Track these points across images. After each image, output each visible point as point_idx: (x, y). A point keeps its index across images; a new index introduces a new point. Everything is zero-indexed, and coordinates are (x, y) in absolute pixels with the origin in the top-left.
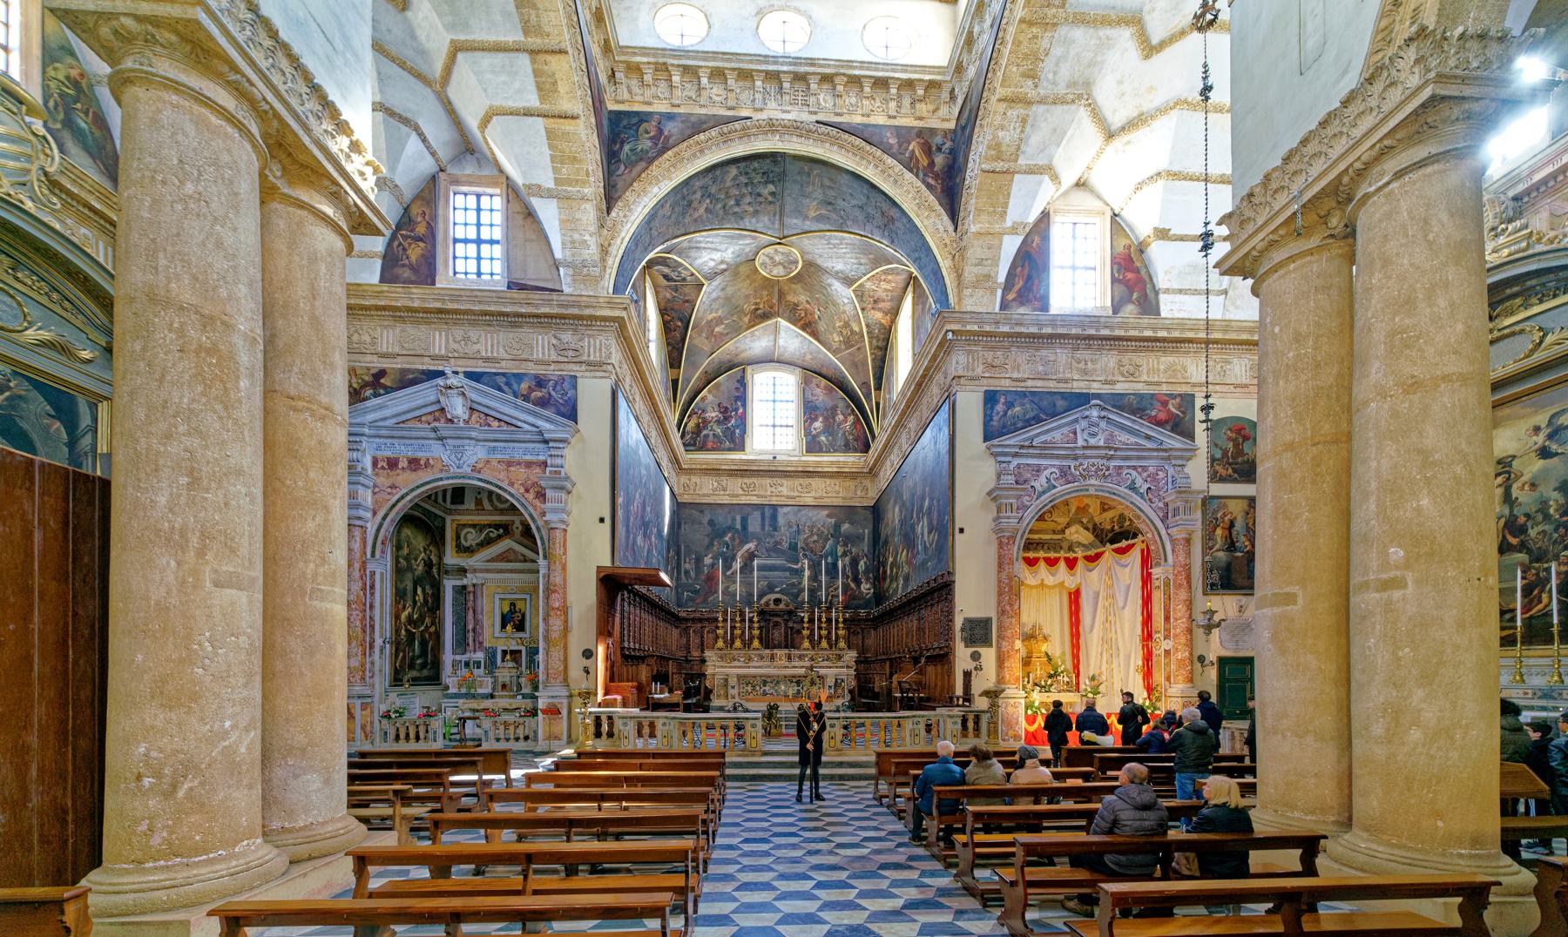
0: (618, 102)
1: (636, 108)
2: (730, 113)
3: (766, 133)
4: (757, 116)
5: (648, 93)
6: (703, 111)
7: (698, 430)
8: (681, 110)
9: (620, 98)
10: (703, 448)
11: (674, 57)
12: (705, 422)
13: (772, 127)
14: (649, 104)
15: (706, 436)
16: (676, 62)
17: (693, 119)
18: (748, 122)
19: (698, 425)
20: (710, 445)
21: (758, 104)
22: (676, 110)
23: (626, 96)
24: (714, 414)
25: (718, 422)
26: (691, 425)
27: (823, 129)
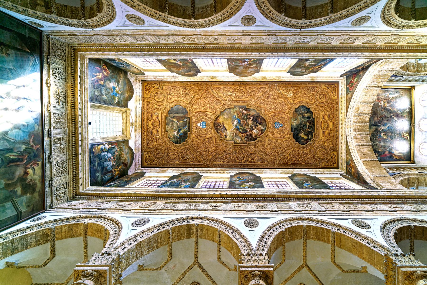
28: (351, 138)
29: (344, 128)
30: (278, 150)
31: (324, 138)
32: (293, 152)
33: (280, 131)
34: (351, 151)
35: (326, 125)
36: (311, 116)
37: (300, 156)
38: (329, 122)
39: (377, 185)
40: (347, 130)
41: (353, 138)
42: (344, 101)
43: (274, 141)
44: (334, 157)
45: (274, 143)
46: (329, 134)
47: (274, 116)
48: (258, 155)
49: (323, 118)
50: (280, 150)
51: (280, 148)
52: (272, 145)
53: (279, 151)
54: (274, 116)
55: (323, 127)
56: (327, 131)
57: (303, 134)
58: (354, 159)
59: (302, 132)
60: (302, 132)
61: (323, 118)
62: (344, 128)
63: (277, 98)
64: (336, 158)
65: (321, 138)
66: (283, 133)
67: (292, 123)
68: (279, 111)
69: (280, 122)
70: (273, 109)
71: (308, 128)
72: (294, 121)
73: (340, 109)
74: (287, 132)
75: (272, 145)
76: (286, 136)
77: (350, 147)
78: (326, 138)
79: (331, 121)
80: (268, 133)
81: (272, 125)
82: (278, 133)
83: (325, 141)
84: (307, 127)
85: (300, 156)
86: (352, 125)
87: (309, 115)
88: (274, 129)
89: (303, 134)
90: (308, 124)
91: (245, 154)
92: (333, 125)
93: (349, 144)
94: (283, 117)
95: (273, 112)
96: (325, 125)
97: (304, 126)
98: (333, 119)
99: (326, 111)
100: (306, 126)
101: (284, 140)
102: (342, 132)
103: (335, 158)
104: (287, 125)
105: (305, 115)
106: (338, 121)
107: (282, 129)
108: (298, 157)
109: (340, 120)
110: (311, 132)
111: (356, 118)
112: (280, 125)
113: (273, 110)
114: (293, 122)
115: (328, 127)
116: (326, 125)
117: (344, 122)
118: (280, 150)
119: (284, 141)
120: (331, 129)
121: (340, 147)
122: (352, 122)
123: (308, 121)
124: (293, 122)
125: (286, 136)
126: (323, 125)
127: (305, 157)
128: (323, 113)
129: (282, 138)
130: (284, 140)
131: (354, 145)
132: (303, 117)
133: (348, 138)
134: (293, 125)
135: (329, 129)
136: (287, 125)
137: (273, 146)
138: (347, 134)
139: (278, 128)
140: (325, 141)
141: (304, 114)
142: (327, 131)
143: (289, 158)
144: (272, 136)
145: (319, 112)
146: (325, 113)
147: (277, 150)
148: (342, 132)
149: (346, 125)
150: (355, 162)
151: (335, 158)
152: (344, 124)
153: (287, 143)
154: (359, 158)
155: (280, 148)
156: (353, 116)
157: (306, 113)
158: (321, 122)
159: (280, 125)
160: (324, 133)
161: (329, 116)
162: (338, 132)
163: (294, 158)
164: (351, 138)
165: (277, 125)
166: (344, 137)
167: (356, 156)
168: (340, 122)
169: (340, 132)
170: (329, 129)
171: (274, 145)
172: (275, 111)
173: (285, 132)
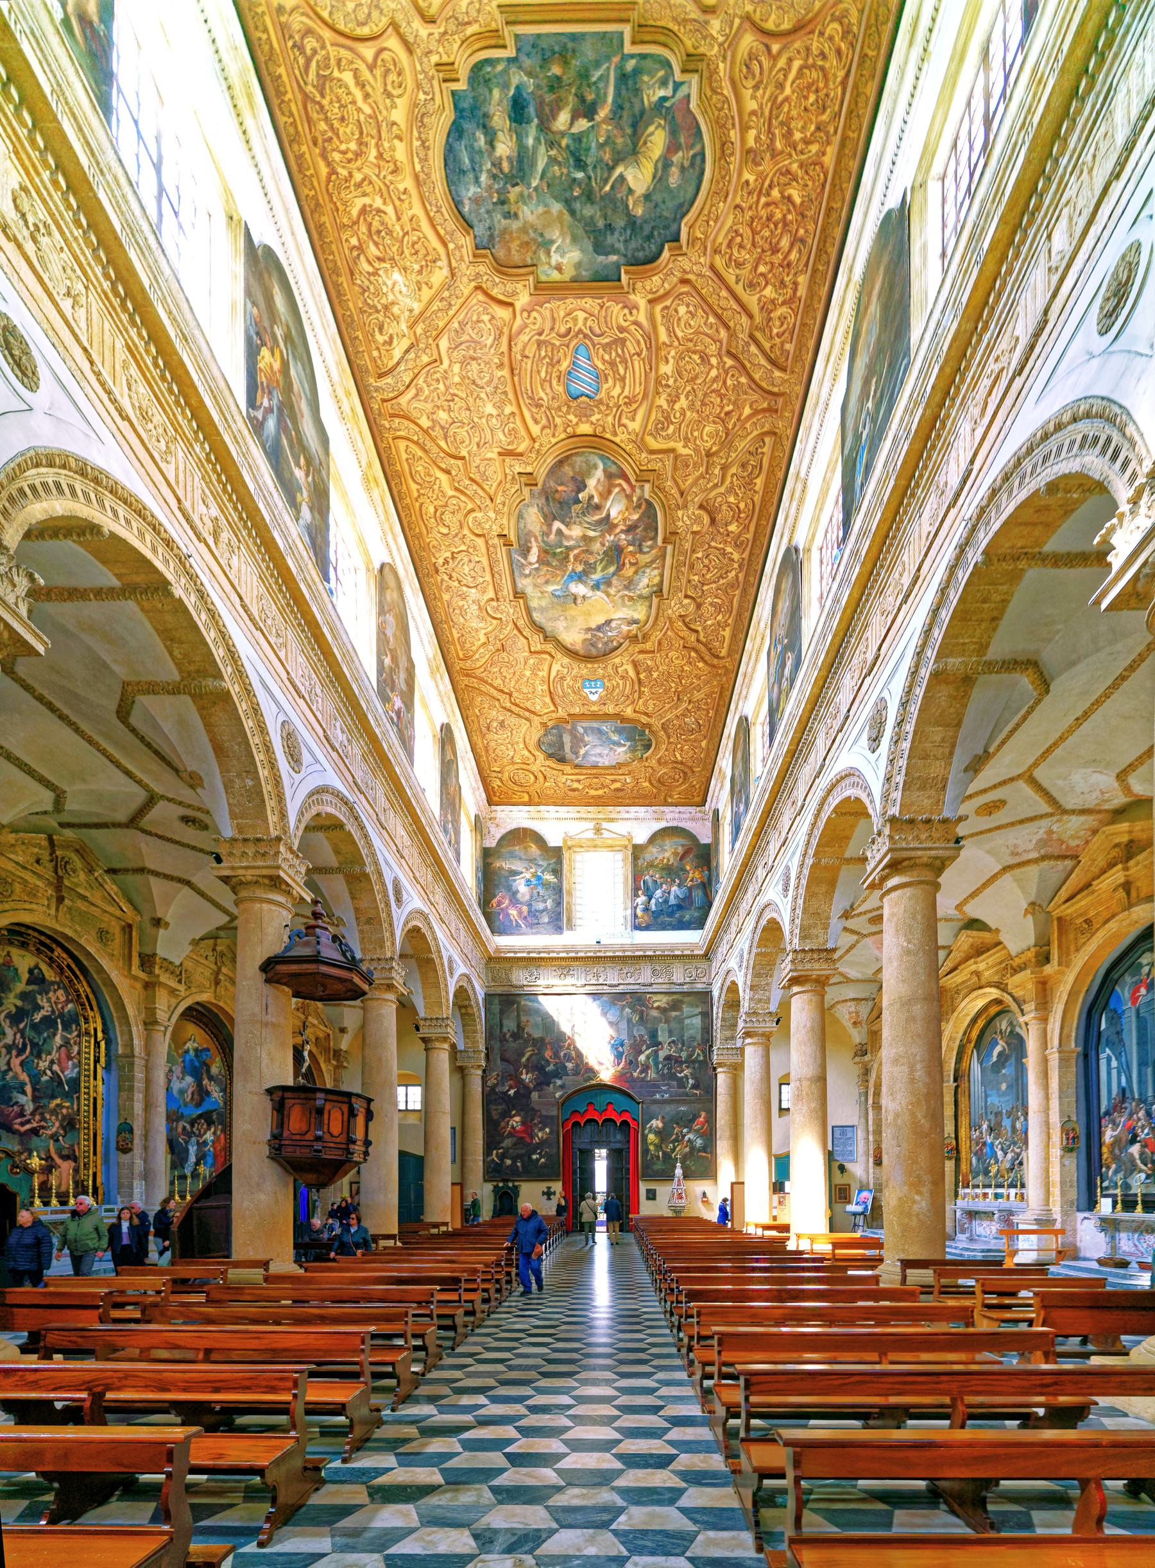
30: (714, 373)
33: (612, 364)
43: (662, 402)
45: (672, 401)
47: (539, 406)
50: (714, 361)
51: (705, 358)
52: (683, 413)
53: (721, 362)
54: (539, 406)
63: (441, 386)
66: (623, 342)
67: (567, 276)
68: (505, 372)
69: (564, 365)
70: (499, 407)
72: (555, 258)
74: (616, 311)
75: (683, 413)
76: (642, 318)
80: (625, 437)
81: (584, 415)
82: (623, 379)
88: (601, 402)
94: (539, 344)
95: (514, 409)
101: (663, 337)
104: (581, 315)
107: (605, 347)
112: (583, 361)
113: (508, 410)
114: (559, 268)
119: (671, 332)
124: (559, 268)
125: (642, 318)
129: (649, 349)
130: (663, 337)
136: (581, 315)
137: (691, 407)
139: (600, 377)
144: (640, 416)
147: (715, 380)
153: (682, 310)
155: (705, 358)
159: (583, 361)
165: (583, 383)
171: (683, 402)
172: (511, 396)
173: (622, 329)
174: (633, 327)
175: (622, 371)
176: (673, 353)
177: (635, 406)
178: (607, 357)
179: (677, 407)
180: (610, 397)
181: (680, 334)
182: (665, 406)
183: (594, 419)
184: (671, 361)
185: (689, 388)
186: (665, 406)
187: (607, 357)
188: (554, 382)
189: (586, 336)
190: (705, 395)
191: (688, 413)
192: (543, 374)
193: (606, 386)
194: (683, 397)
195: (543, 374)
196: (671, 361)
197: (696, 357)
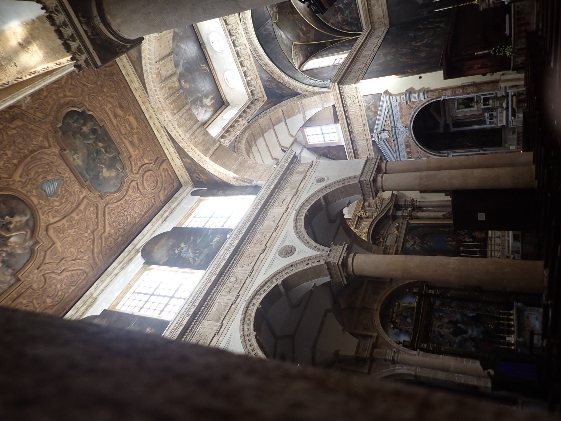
0: (264, 96)
1: (263, 90)
2: (251, 56)
3: (251, 41)
4: (248, 47)
5: (257, 87)
6: (255, 66)
7: (349, 24)
8: (258, 74)
9: (262, 96)
10: (358, 19)
11: (244, 81)
12: (344, 20)
13: (249, 40)
14: (260, 86)
15: (351, 18)
16: (245, 80)
17: (259, 69)
18: (252, 49)
19: (347, 25)
20: (355, 15)
21: (244, 47)
22: (258, 76)
23: (260, 94)
24: (339, 17)
25: (342, 14)
26: (347, 28)
27: (242, 19)
28: (175, 128)
29: (154, 116)
30: (86, 235)
31: (137, 152)
32: (113, 216)
34: (186, 150)
35: (127, 126)
36: (95, 125)
37: (126, 213)
38: (127, 117)
39: (242, 181)
40: (161, 119)
41: (177, 127)
42: (128, 65)
44: (166, 173)
46: (140, 140)
48: (59, 278)
49: (116, 116)
50: (89, 231)
51: (87, 227)
52: (69, 235)
55: (126, 134)
56: (135, 136)
57: (104, 170)
58: (195, 159)
59: (102, 168)
60: (102, 168)
61: (116, 116)
62: (154, 116)
64: (170, 172)
65: (134, 156)
71: (106, 152)
73: (129, 83)
76: (81, 197)
77: (181, 145)
78: (141, 150)
79: (129, 115)
82: (62, 203)
83: (142, 157)
84: (103, 151)
85: (126, 213)
86: (164, 106)
87: (90, 124)
89: (104, 170)
90: (101, 144)
91: (32, 302)
92: (136, 119)
93: (177, 141)
96: (126, 127)
97: (97, 153)
98: (129, 108)
99: (111, 100)
100: (101, 151)
102: (154, 124)
103: (168, 174)
105: (85, 129)
106: (138, 108)
108: (124, 218)
109: (141, 103)
110: (115, 157)
111: (163, 90)
115: (132, 128)
116: (127, 126)
117: (149, 105)
118: (89, 231)
120: (137, 128)
121: (166, 151)
122: (162, 101)
123: (97, 139)
126: (123, 131)
127: (133, 207)
128: (110, 106)
131: (186, 139)
132: (85, 136)
133: (168, 130)
134: (79, 166)
135: (135, 131)
138: (165, 124)
140: (142, 157)
141: (81, 129)
142: (135, 136)
143: (113, 231)
145: (102, 107)
146: (112, 104)
147: (86, 237)
148: (154, 124)
149: (156, 109)
150: (201, 164)
151: (168, 174)
152: (150, 108)
153: (92, 209)
154: (203, 156)
155: (87, 227)
156: (158, 89)
157: (84, 125)
158: (118, 126)
160: (131, 143)
161: (121, 107)
162: (149, 128)
163: (119, 224)
164: (175, 128)
166: (163, 132)
167: (196, 155)
168: (143, 108)
169: (152, 125)
170: (135, 131)
174: (77, 196)
175: (64, 201)
176: (81, 215)
177: (57, 215)
178: (63, 192)
179: (69, 231)
180: (53, 202)
181: (87, 213)
182: (66, 226)
183: (41, 201)
184: (79, 217)
185: (76, 230)
186: (66, 226)
187: (63, 192)
188: (41, 177)
189: (63, 180)
190: (79, 238)
191: (70, 237)
192: (40, 170)
193: (55, 198)
194: (73, 230)
195: (40, 170)
196: (79, 217)
197: (86, 224)
